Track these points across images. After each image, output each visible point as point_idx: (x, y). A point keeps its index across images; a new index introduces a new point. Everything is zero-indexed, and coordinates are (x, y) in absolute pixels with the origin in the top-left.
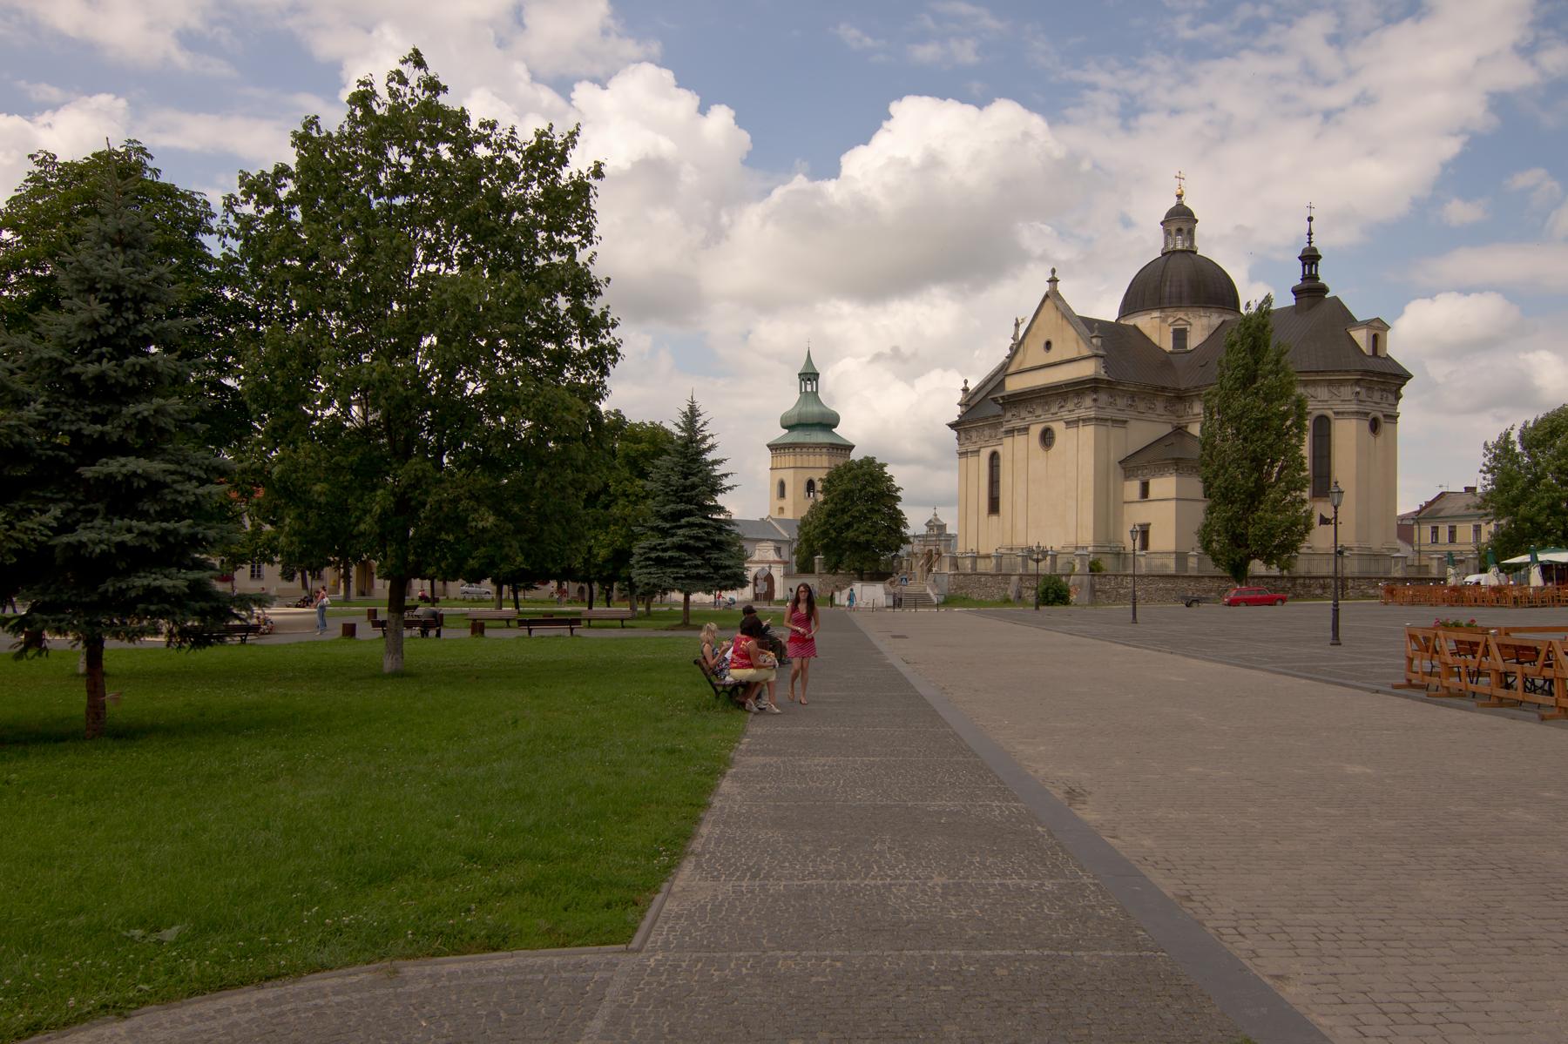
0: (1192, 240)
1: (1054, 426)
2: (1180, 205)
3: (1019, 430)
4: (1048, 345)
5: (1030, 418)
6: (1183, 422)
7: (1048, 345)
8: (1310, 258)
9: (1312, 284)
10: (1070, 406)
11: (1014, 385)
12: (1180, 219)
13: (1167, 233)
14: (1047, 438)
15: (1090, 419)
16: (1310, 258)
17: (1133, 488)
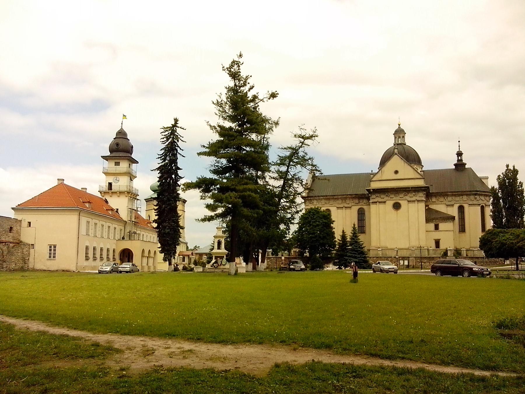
0: (404, 140)
1: (400, 202)
2: (399, 127)
3: (380, 202)
4: (396, 172)
5: (386, 198)
6: (428, 204)
7: (396, 172)
8: (459, 154)
9: (460, 163)
10: (410, 195)
11: (374, 185)
12: (399, 133)
13: (395, 138)
14: (397, 206)
15: (422, 201)
16: (459, 154)
17: (432, 226)
